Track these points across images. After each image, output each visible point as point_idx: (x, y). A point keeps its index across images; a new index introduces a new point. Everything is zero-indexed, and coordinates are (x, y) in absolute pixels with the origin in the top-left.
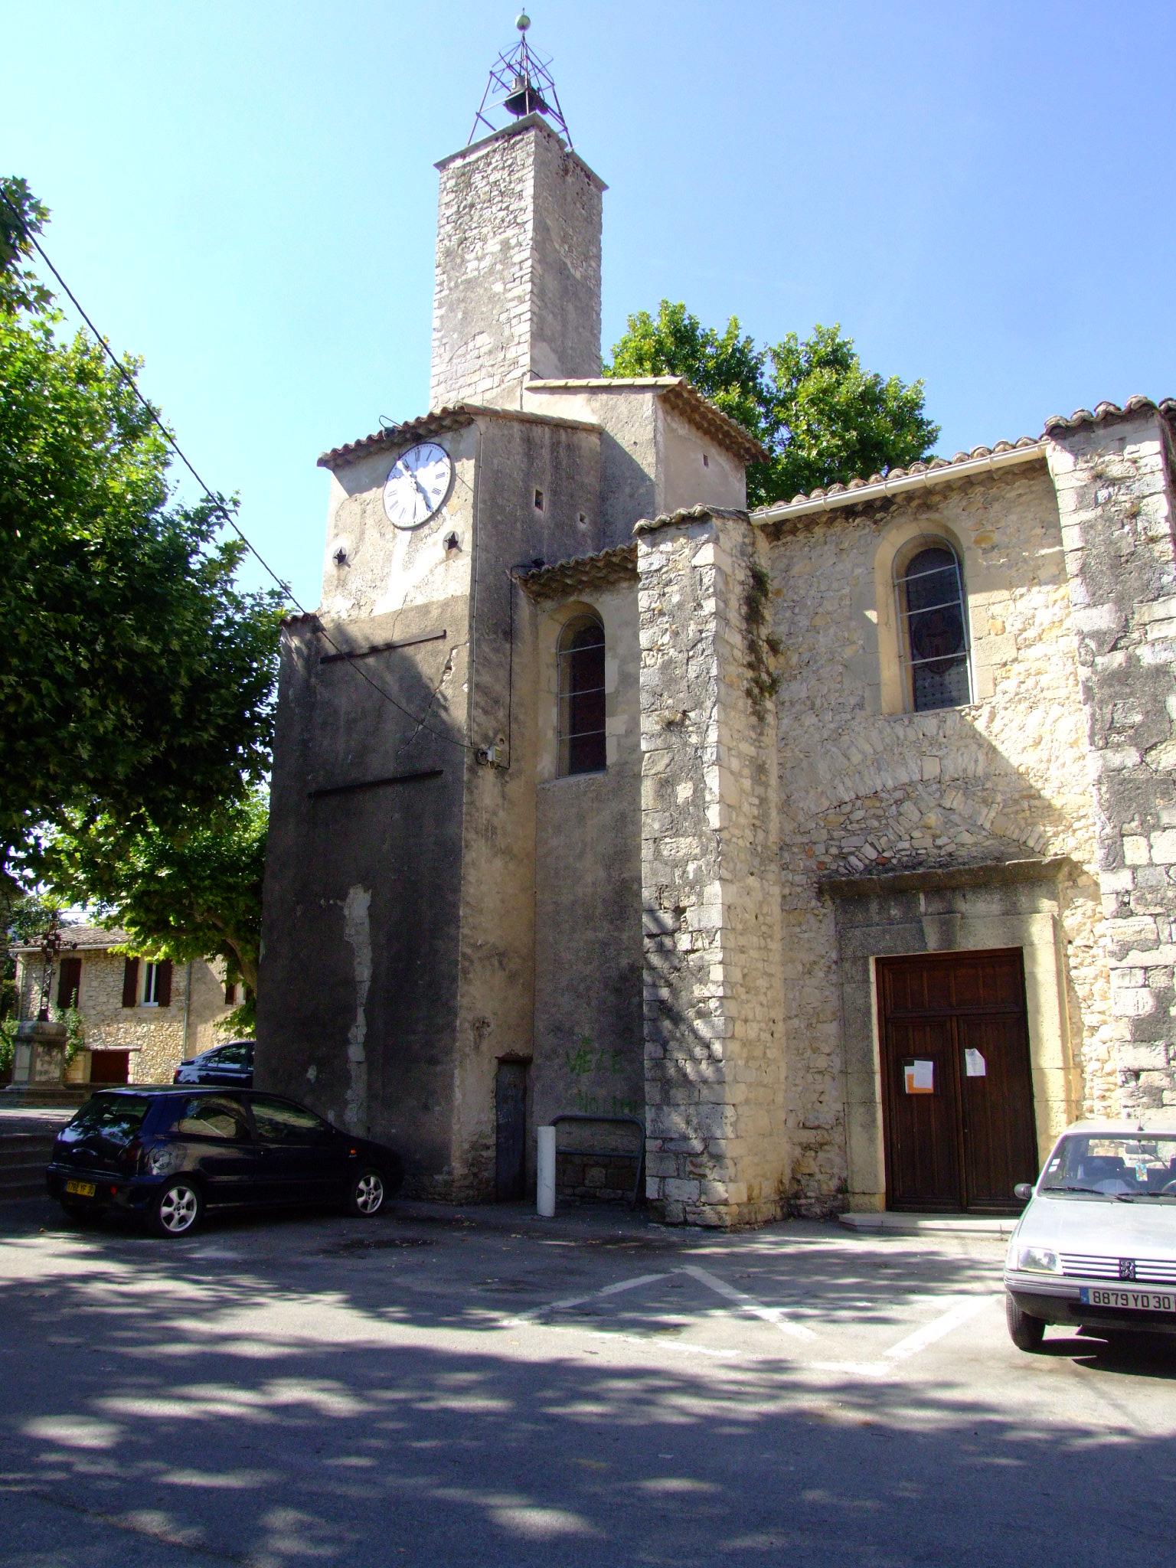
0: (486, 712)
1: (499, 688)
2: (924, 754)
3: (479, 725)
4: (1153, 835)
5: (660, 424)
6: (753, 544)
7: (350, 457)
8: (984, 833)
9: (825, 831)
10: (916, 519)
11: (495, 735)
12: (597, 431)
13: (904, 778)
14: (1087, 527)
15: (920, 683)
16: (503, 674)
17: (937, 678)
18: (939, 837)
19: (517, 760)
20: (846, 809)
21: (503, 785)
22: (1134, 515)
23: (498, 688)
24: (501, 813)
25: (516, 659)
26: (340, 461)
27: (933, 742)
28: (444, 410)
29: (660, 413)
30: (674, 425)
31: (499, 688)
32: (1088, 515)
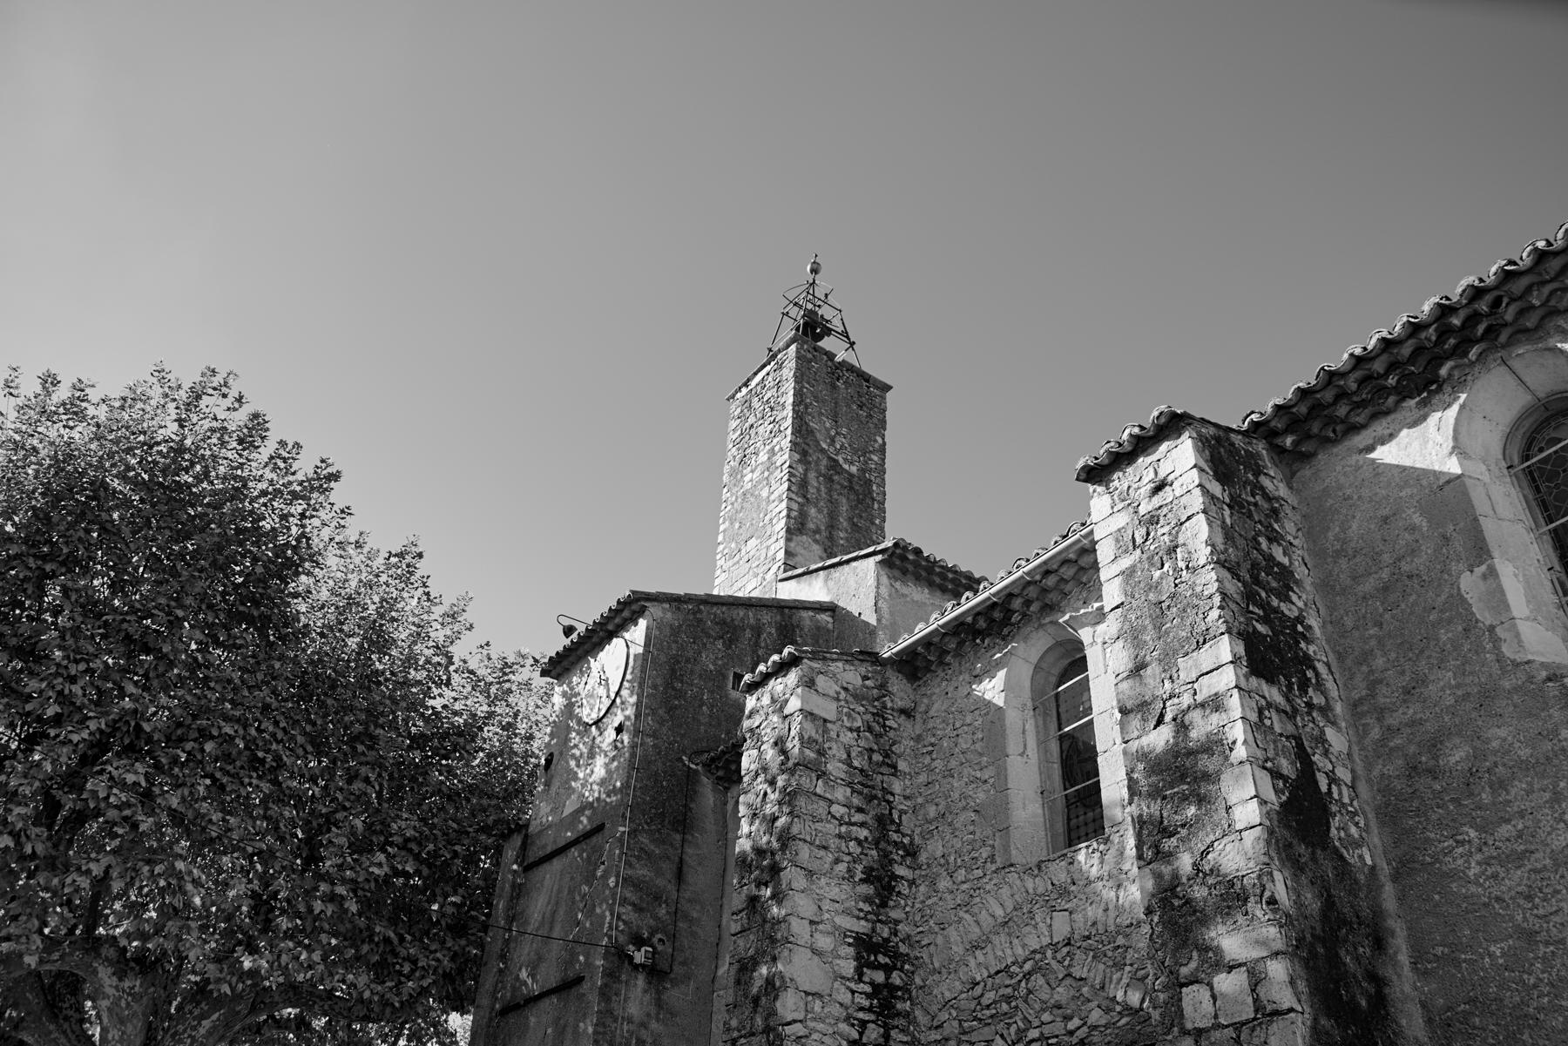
0: (638, 909)
1: (664, 883)
2: (1053, 909)
3: (625, 923)
4: (1216, 980)
5: (884, 591)
6: (882, 686)
7: (565, 663)
8: (1118, 1008)
9: (955, 1023)
10: (1041, 626)
11: (652, 935)
12: (831, 608)
13: (1034, 944)
14: (1128, 574)
15: (1074, 822)
16: (668, 868)
17: (1090, 815)
18: (1071, 1018)
19: (684, 963)
20: (978, 990)
21: (658, 992)
22: (1172, 550)
23: (660, 882)
24: (654, 1025)
25: (689, 851)
26: (559, 669)
27: (1064, 893)
28: (619, 602)
29: (884, 580)
30: (905, 590)
31: (664, 883)
32: (1126, 562)
